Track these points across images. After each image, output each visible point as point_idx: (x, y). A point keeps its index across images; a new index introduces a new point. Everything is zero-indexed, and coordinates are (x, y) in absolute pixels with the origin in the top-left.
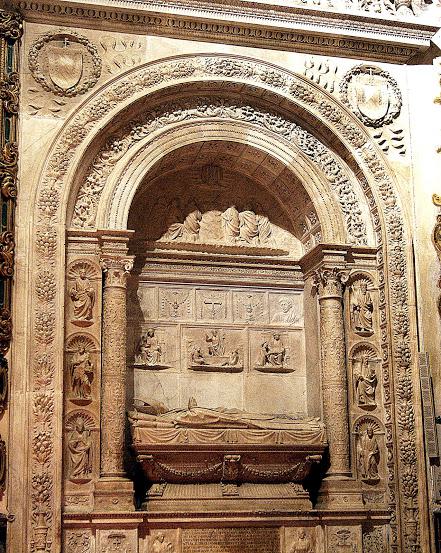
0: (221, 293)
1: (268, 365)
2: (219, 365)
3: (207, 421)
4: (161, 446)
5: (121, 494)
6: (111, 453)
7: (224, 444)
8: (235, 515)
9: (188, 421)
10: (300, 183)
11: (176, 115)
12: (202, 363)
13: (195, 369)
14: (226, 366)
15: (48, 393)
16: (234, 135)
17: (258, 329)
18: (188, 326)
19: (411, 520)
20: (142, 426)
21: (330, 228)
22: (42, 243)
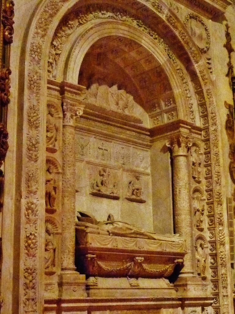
0: (108, 143)
1: (134, 197)
2: (108, 193)
3: (128, 232)
4: (102, 248)
5: (78, 284)
6: (69, 252)
7: (137, 249)
8: (136, 300)
9: (116, 231)
10: (166, 78)
11: (103, 14)
12: (99, 191)
13: (94, 195)
14: (112, 195)
15: (35, 201)
16: (136, 37)
17: (128, 171)
18: (88, 163)
19: (226, 303)
20: (91, 233)
21: (182, 110)
22: (32, 82)
